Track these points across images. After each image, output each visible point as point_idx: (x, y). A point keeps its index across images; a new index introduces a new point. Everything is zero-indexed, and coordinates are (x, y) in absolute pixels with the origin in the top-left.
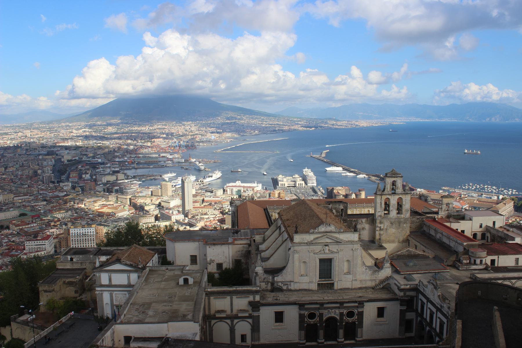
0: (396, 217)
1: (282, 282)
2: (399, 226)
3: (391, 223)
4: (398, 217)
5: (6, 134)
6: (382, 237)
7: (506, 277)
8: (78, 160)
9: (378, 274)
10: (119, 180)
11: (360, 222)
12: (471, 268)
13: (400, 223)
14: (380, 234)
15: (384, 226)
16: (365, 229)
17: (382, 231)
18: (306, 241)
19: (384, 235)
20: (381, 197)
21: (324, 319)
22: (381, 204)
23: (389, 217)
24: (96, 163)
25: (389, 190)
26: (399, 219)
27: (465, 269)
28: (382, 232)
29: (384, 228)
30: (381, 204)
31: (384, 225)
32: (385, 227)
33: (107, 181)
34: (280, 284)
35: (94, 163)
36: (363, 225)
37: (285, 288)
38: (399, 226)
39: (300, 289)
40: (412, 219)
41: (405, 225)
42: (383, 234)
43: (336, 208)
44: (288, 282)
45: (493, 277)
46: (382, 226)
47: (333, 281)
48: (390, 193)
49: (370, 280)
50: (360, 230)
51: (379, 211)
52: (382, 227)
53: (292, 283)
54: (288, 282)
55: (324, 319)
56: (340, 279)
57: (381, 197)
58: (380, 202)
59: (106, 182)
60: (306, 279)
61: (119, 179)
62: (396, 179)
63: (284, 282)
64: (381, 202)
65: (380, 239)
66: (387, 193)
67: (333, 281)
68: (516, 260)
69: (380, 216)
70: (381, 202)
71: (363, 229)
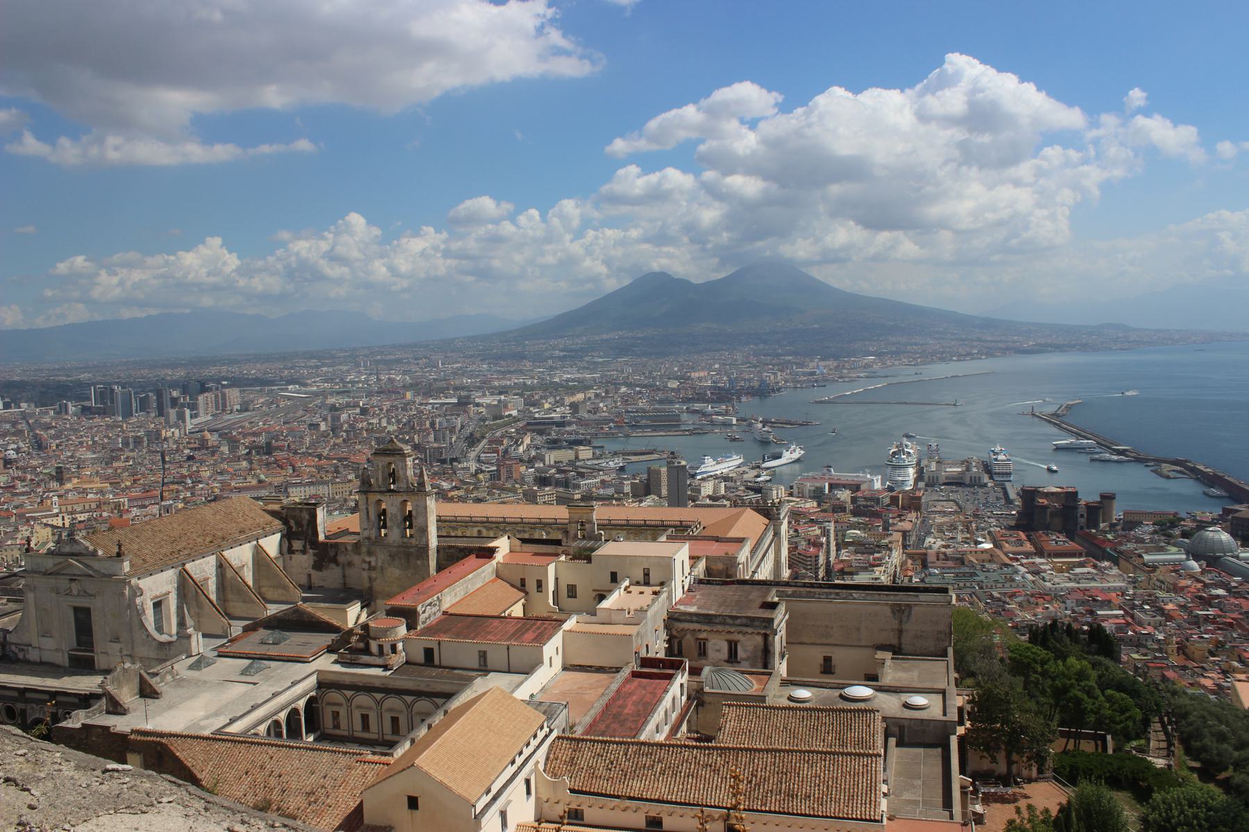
0: (401, 543)
1: (16, 644)
2: (408, 562)
3: (390, 556)
4: (403, 543)
5: (399, 361)
6: (374, 584)
7: (390, 687)
8: (515, 417)
9: (170, 649)
10: (579, 461)
11: (343, 549)
12: (361, 661)
13: (408, 556)
14: (370, 579)
15: (377, 561)
16: (354, 565)
17: (374, 572)
18: (43, 570)
19: (378, 581)
20: (367, 498)
21: (29, 722)
22: (368, 513)
23: (386, 542)
24: (548, 424)
25: (380, 483)
26: (407, 547)
27: (349, 661)
28: (373, 575)
29: (377, 564)
30: (368, 513)
31: (377, 558)
32: (380, 564)
33: (556, 462)
34: (13, 648)
35: (544, 424)
36: (348, 557)
37: (21, 656)
38: (408, 562)
39: (43, 660)
40: (447, 551)
41: (419, 562)
42: (376, 578)
43: (295, 516)
44: (25, 645)
45: (361, 684)
46: (373, 559)
47: (93, 651)
48: (382, 489)
49: (157, 659)
50: (343, 566)
51: (366, 527)
52: (373, 564)
53: (30, 648)
54: (25, 645)
55: (29, 722)
56: (103, 651)
57: (367, 498)
58: (364, 507)
59: (552, 463)
60: (48, 643)
61: (580, 458)
62: (393, 459)
63: (19, 645)
64: (367, 509)
65: (371, 588)
66: (377, 489)
67: (93, 651)
68: (480, 657)
69: (369, 538)
70: (367, 509)
71: (350, 564)
